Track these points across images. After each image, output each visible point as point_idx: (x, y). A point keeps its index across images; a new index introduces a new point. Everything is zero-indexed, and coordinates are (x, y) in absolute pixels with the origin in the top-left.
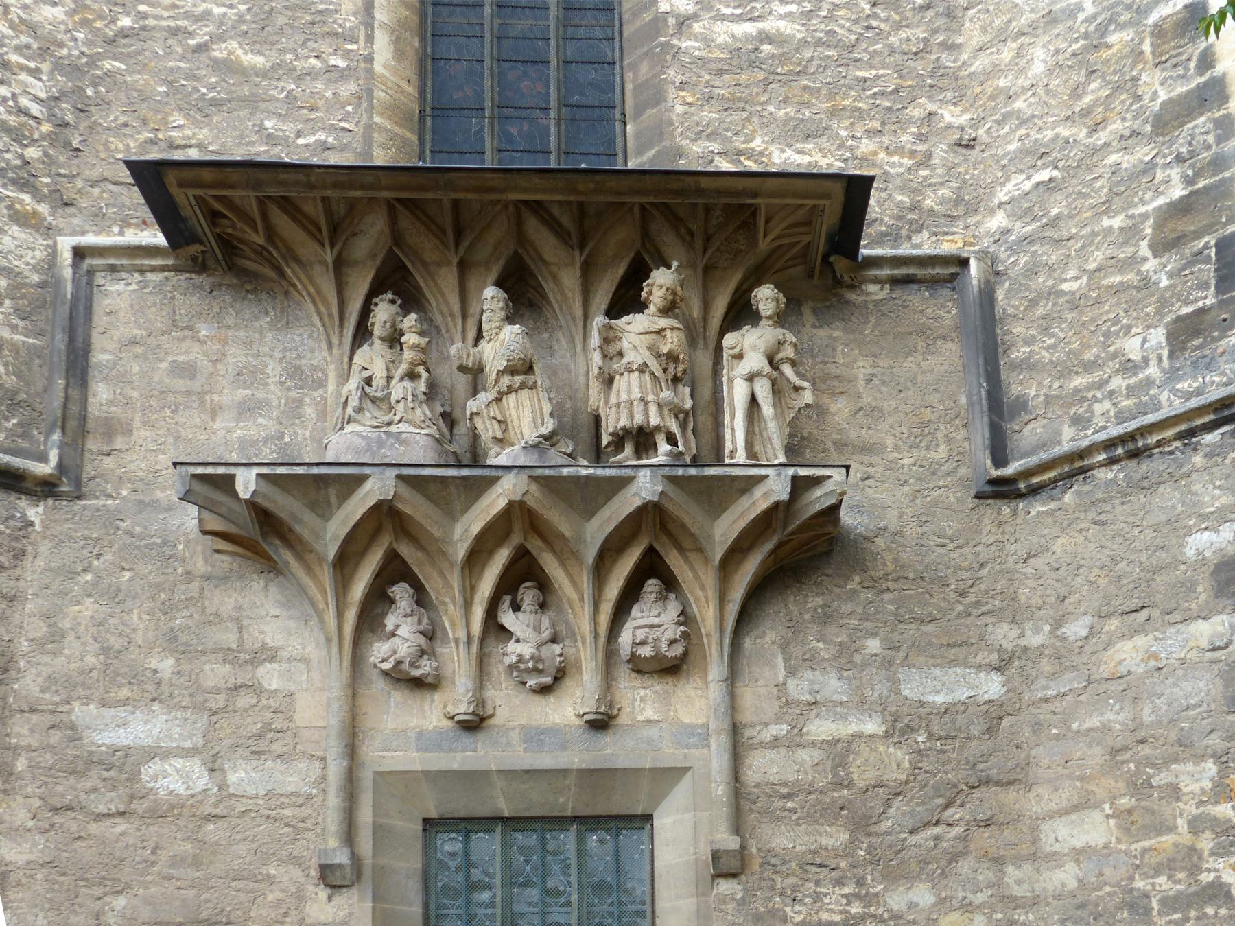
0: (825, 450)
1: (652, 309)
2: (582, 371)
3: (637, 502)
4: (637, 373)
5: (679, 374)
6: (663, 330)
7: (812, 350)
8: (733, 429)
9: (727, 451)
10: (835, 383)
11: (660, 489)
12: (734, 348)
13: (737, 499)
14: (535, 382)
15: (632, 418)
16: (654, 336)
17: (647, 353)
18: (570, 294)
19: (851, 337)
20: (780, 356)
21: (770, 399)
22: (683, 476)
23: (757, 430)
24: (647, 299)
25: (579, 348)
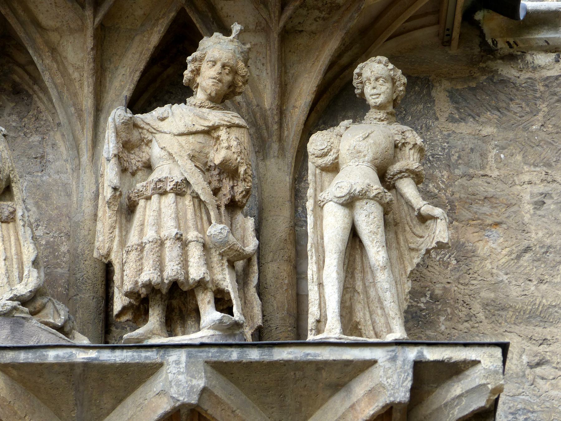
0: (470, 317)
1: (200, 96)
2: (88, 194)
3: (165, 406)
4: (171, 196)
5: (238, 197)
6: (215, 128)
7: (449, 155)
8: (320, 285)
9: (311, 321)
10: (486, 209)
11: (201, 383)
12: (325, 155)
13: (325, 400)
14: (14, 212)
15: (160, 266)
16: (200, 138)
17: (190, 165)
18: (76, 75)
19: (511, 135)
20: (396, 167)
21: (380, 236)
22: (238, 363)
23: (359, 285)
24: (192, 81)
25: (85, 158)
